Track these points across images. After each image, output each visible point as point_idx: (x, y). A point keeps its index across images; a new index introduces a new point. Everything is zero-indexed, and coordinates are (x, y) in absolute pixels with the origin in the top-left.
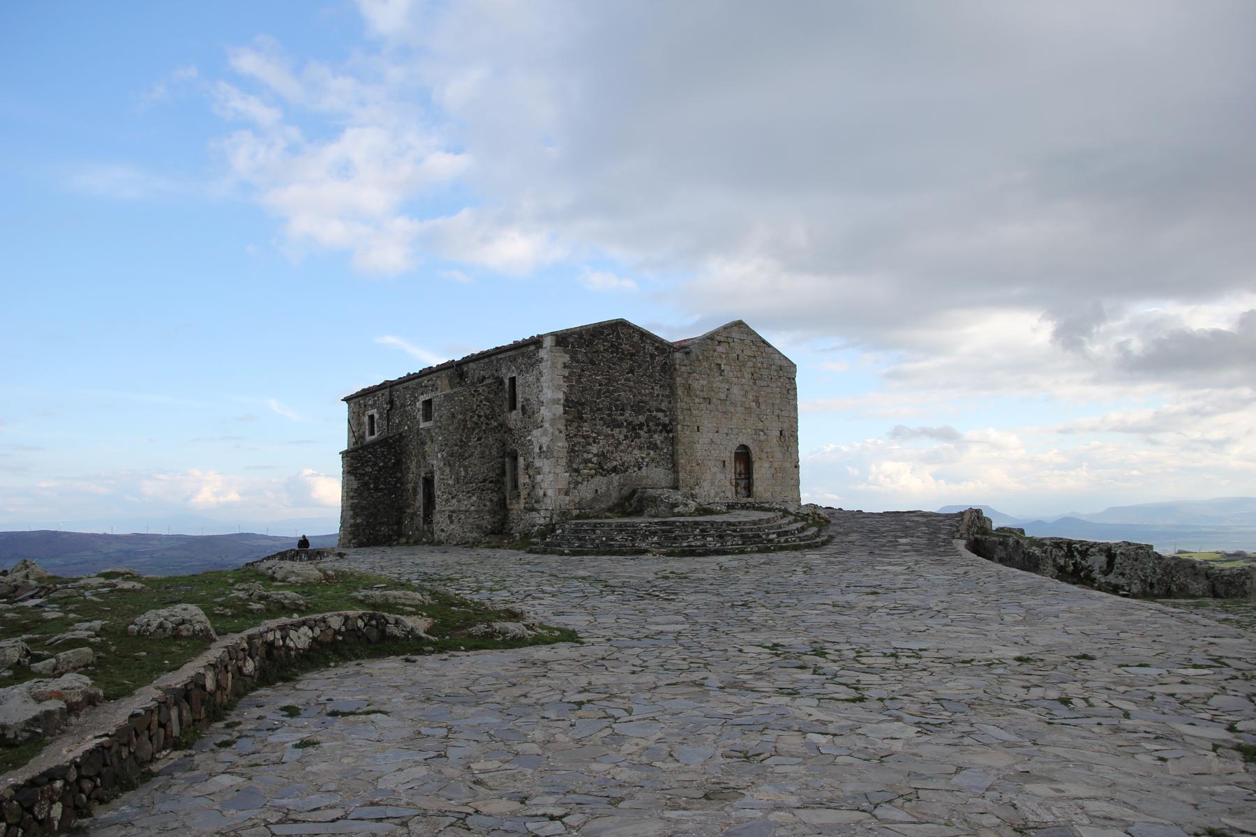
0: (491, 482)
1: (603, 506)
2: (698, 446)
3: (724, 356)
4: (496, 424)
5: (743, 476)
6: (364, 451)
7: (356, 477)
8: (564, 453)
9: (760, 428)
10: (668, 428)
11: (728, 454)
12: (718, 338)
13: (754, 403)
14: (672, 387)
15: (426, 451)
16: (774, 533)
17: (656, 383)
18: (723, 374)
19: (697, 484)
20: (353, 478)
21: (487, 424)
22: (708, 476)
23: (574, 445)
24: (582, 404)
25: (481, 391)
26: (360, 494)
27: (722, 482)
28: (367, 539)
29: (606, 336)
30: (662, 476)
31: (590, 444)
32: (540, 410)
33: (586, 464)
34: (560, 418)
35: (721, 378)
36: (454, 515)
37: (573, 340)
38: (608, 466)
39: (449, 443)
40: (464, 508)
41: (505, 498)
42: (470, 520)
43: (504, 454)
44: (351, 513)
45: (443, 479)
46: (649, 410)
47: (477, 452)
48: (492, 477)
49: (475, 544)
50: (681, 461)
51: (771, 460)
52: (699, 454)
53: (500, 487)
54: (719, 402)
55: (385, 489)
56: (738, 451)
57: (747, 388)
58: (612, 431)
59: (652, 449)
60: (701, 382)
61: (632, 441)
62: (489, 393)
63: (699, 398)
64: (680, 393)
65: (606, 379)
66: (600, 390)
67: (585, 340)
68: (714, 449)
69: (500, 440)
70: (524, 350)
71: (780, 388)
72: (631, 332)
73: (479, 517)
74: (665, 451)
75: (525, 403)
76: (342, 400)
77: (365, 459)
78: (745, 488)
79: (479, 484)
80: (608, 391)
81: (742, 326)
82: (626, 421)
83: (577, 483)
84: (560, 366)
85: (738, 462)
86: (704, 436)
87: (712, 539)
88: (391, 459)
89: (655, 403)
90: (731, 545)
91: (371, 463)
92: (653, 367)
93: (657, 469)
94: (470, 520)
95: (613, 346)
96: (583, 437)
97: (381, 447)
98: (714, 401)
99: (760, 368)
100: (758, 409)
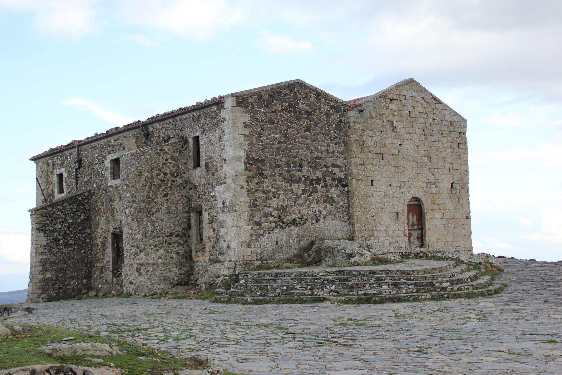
0: (178, 236)
1: (283, 257)
2: (372, 199)
3: (396, 113)
4: (181, 181)
5: (416, 227)
6: (53, 208)
7: (45, 233)
8: (246, 208)
9: (432, 181)
10: (344, 183)
11: (401, 206)
12: (391, 96)
13: (426, 158)
14: (346, 144)
15: (114, 208)
16: (447, 281)
17: (331, 140)
19: (372, 235)
20: (42, 234)
21: (173, 181)
22: (382, 227)
23: (255, 200)
24: (263, 161)
25: (166, 150)
26: (50, 250)
27: (396, 233)
28: (56, 293)
29: (283, 97)
30: (339, 228)
31: (271, 199)
32: (222, 167)
33: (267, 217)
34: (241, 174)
36: (143, 268)
37: (252, 101)
38: (289, 218)
39: (137, 200)
40: (151, 261)
41: (191, 251)
42: (158, 273)
43: (189, 209)
44: (41, 268)
45: (131, 234)
46: (325, 166)
47: (163, 208)
48: (179, 231)
49: (164, 295)
50: (357, 213)
51: (443, 211)
52: (373, 207)
53: (186, 241)
54: (392, 157)
55: (75, 244)
56: (410, 203)
57: (418, 143)
58: (291, 186)
61: (310, 195)
62: (174, 151)
63: (373, 154)
64: (354, 149)
65: (284, 137)
66: (279, 148)
67: (264, 100)
68: (388, 202)
69: (185, 196)
70: (207, 110)
72: (307, 92)
73: (166, 269)
74: (341, 204)
75: (208, 161)
76: (30, 160)
77: (55, 216)
78: (418, 238)
79: (166, 238)
80: (286, 148)
81: (414, 84)
82: (304, 176)
83: (259, 235)
84: (241, 125)
85: (410, 214)
87: (386, 287)
88: (80, 216)
89: (330, 159)
90: (406, 293)
91: (61, 220)
92: (328, 125)
93: (334, 221)
94: (158, 273)
95: (290, 105)
96: (264, 192)
97: (69, 204)
98: (387, 156)
99: (431, 124)
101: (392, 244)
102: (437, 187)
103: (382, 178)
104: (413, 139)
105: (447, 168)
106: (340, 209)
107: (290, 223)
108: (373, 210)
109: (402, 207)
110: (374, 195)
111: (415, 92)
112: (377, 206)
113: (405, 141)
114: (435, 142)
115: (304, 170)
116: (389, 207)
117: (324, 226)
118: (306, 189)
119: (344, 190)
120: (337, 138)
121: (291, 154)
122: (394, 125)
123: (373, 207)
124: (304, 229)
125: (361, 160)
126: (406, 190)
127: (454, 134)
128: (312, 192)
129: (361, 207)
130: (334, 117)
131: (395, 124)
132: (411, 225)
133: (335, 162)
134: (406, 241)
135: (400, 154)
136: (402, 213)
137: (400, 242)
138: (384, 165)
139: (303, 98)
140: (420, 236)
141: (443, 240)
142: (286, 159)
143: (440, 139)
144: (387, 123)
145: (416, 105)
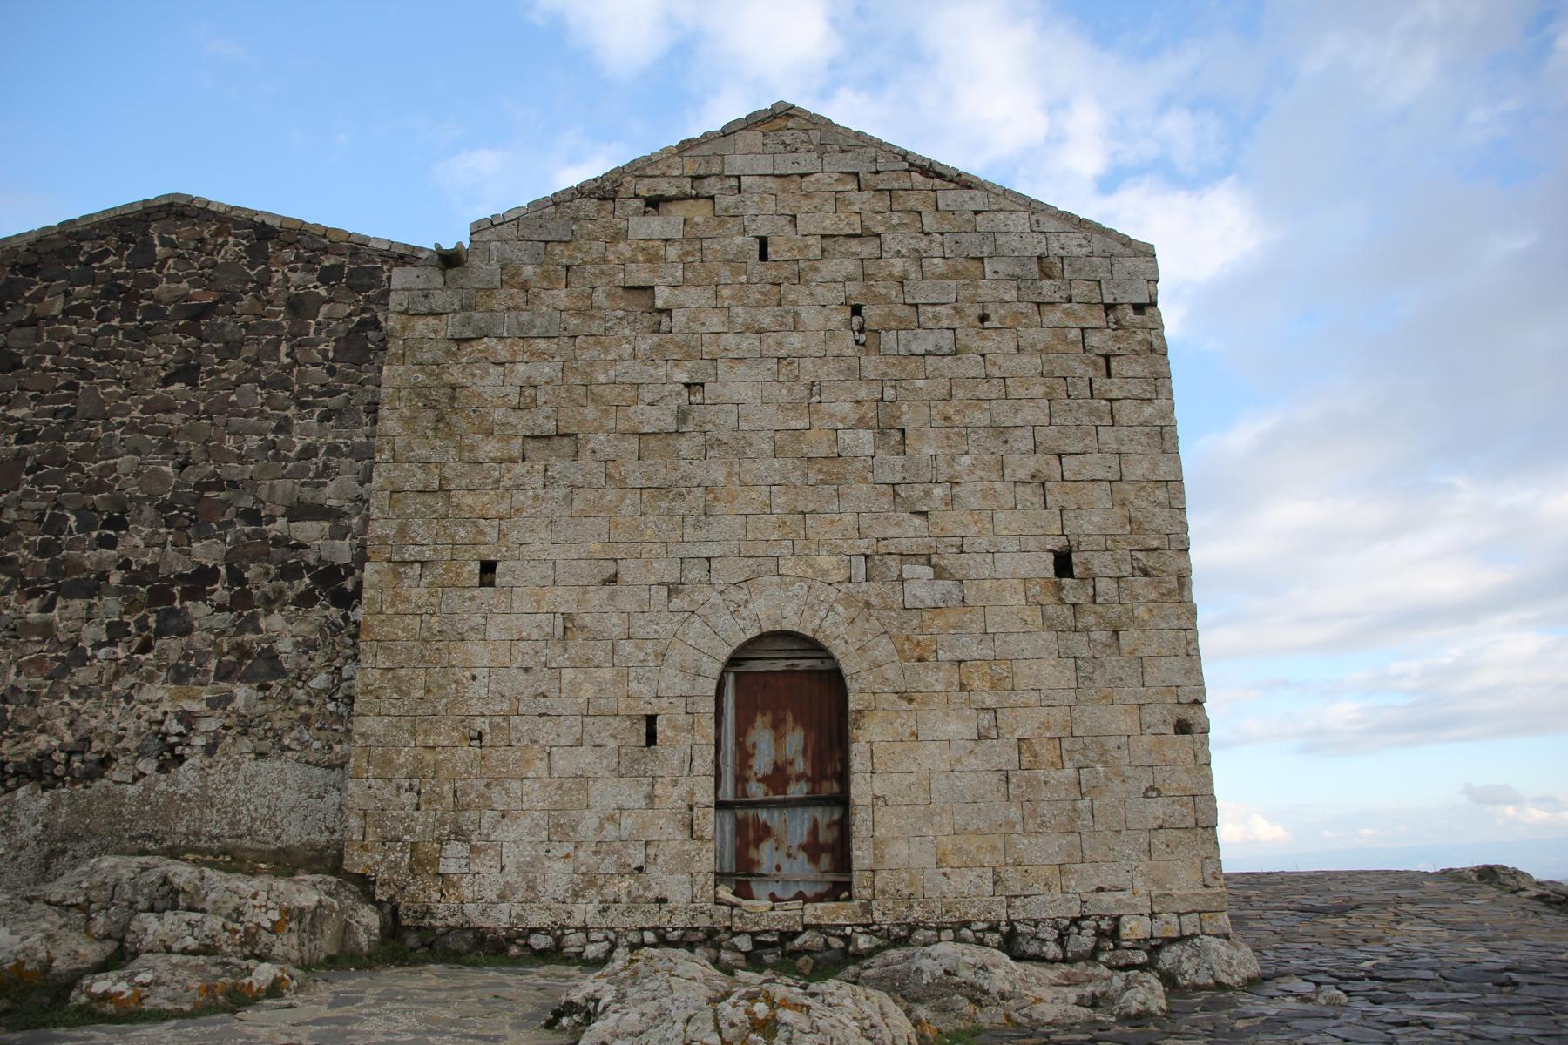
5: (797, 790)
9: (906, 546)
11: (674, 682)
13: (866, 436)
17: (302, 405)
19: (459, 834)
22: (533, 792)
27: (628, 822)
29: (87, 263)
30: (289, 797)
35: (648, 342)
46: (252, 517)
51: (990, 700)
57: (809, 369)
58: (48, 607)
59: (245, 679)
60: (521, 368)
61: (145, 648)
65: (55, 414)
68: (585, 664)
71: (1046, 351)
72: (206, 234)
74: (320, 681)
78: (813, 849)
80: (56, 457)
82: (125, 565)
85: (761, 721)
89: (283, 486)
92: (293, 348)
95: (113, 290)
98: (599, 441)
100: (899, 460)
101: (592, 883)
102: (952, 577)
103: (557, 548)
104: (782, 353)
105: (1022, 474)
106: (311, 704)
107: (16, 774)
108: (477, 707)
110: (493, 633)
111: (802, 157)
112: (506, 688)
113: (721, 365)
114: (930, 360)
115: (134, 540)
116: (588, 690)
117: (205, 787)
118: (126, 618)
119: (346, 618)
120: (339, 393)
121: (75, 480)
122: (659, 304)
123: (479, 689)
124: (83, 803)
125: (429, 473)
126: (716, 598)
127: (1066, 313)
128: (160, 633)
129: (399, 690)
130: (338, 311)
131: (662, 296)
132: (765, 780)
133: (307, 495)
134: (697, 866)
136: (682, 719)
138: (573, 487)
139: (180, 256)
140: (825, 836)
141: (987, 859)
142: (43, 499)
143: (964, 340)
144: (610, 296)
145: (806, 205)
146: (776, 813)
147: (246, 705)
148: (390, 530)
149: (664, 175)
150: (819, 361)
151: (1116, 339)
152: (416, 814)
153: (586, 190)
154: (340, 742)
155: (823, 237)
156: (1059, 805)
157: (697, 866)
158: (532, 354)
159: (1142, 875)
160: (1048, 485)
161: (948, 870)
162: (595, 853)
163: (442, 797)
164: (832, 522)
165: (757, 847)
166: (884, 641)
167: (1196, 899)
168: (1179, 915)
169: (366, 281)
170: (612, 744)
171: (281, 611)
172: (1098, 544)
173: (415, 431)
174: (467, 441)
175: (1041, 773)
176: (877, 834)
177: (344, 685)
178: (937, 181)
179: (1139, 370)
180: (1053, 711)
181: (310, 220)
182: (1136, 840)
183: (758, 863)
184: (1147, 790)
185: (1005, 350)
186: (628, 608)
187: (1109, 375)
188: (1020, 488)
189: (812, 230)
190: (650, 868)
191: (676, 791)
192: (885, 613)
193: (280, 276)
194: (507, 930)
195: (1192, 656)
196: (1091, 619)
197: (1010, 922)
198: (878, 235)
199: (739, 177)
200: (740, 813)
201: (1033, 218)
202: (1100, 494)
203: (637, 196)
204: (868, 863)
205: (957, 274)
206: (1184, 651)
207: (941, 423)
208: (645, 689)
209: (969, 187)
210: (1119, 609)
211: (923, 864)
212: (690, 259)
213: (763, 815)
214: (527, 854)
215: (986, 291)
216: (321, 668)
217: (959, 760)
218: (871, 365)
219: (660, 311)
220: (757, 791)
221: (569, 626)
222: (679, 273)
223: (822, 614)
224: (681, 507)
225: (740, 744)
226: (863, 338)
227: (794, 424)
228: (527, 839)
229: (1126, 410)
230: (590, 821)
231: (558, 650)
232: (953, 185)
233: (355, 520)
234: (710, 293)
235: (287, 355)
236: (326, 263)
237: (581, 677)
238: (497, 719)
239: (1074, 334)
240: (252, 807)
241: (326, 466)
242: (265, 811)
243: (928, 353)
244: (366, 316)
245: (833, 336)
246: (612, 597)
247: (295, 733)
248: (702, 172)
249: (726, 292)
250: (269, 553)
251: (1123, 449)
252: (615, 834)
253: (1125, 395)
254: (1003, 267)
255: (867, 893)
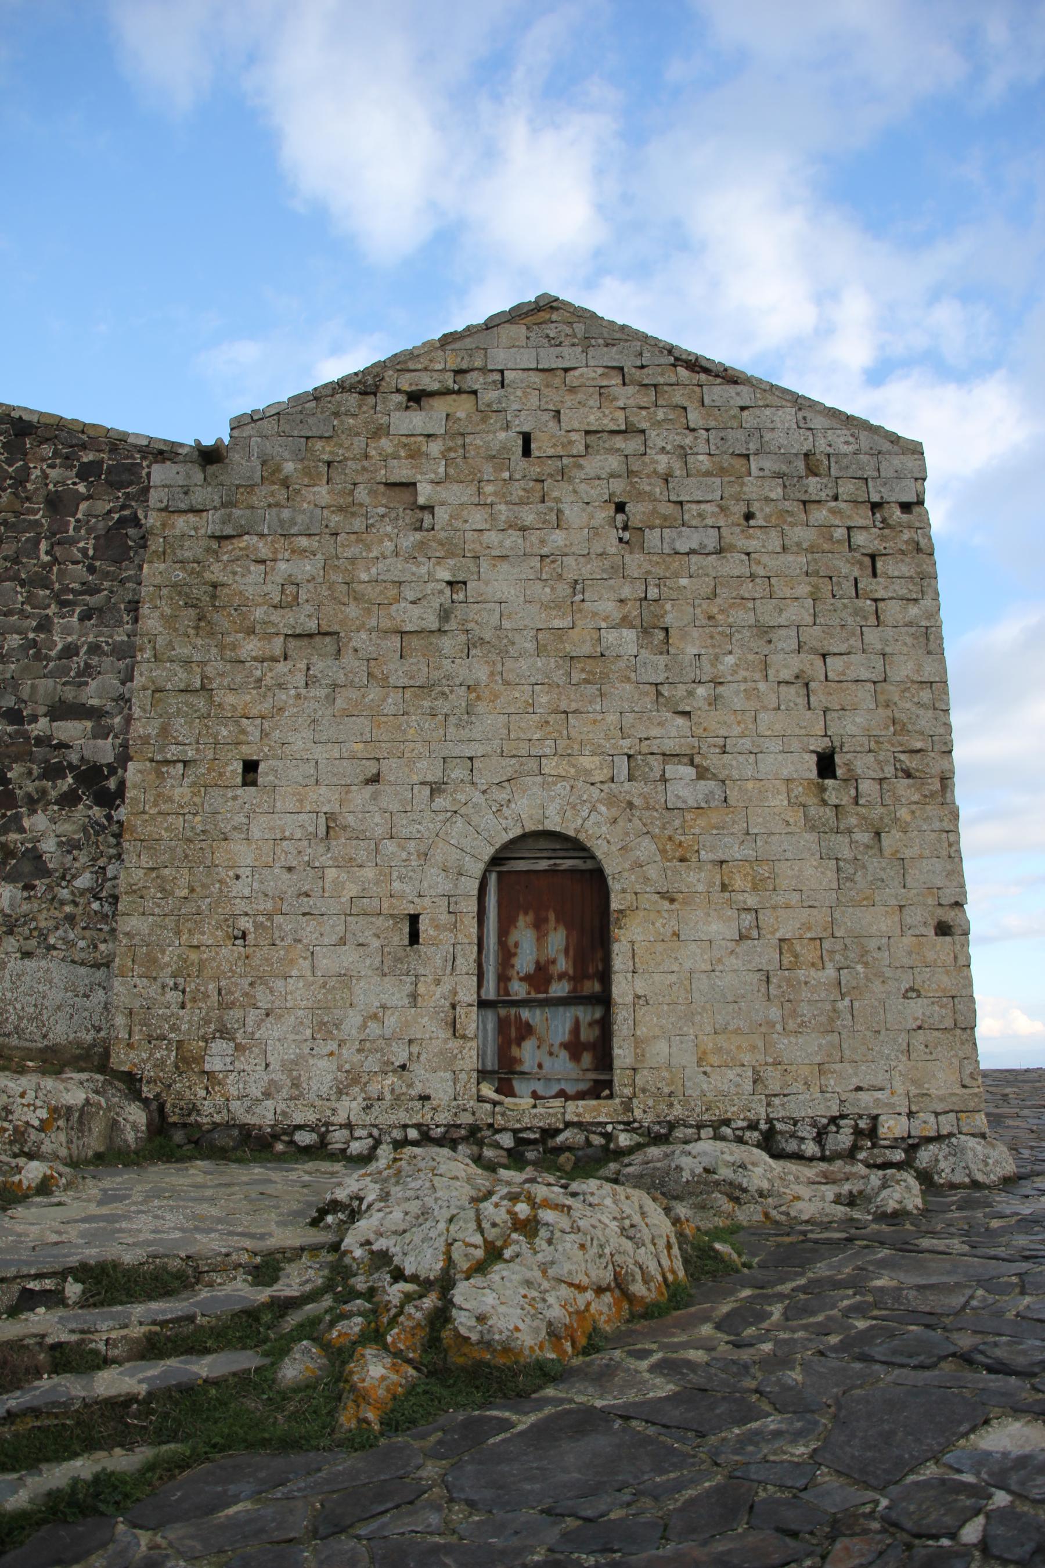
5: (559, 989)
11: (436, 882)
12: (406, 382)
13: (629, 635)
17: (63, 604)
18: (427, 519)
19: (224, 1033)
27: (391, 1021)
30: (56, 996)
35: (410, 540)
51: (751, 901)
57: (572, 568)
60: (282, 566)
68: (348, 863)
71: (811, 550)
74: (84, 881)
78: (574, 1048)
85: (523, 921)
86: (285, 802)
89: (46, 685)
92: (52, 545)
93: (30, 964)
98: (361, 639)
100: (662, 659)
101: (355, 1081)
104: (545, 551)
105: (786, 675)
106: (76, 904)
108: (241, 906)
109: (444, 885)
110: (256, 833)
111: (566, 351)
112: (270, 887)
113: (485, 564)
114: (694, 558)
116: (352, 890)
119: (109, 817)
120: (99, 591)
122: (421, 501)
123: (241, 888)
125: (190, 672)
126: (478, 798)
127: (833, 511)
129: (163, 890)
131: (425, 493)
132: (527, 979)
133: (69, 694)
134: (459, 1064)
135: (452, 625)
136: (444, 918)
137: (417, 1070)
138: (335, 686)
140: (587, 1035)
141: (747, 1058)
144: (372, 493)
145: (569, 400)
146: (538, 1012)
147: (11, 905)
148: (152, 730)
149: (426, 369)
150: (582, 559)
151: (883, 538)
152: (181, 1012)
153: (347, 385)
154: (105, 941)
155: (587, 432)
156: (819, 1005)
157: (459, 1064)
158: (293, 552)
159: (901, 1075)
160: (812, 685)
161: (708, 1069)
162: (359, 1051)
163: (206, 996)
164: (595, 721)
165: (519, 1045)
166: (646, 841)
167: (954, 1099)
168: (937, 1114)
169: (125, 477)
170: (376, 943)
171: (44, 811)
172: (862, 745)
173: (176, 630)
174: (228, 639)
175: (801, 974)
176: (638, 1033)
177: (109, 884)
178: (703, 377)
179: (905, 569)
180: (815, 912)
181: (68, 415)
182: (895, 1040)
183: (520, 1062)
184: (907, 991)
185: (770, 548)
186: (391, 807)
187: (875, 575)
188: (783, 688)
189: (576, 426)
190: (413, 1066)
191: (439, 991)
192: (647, 813)
193: (38, 472)
194: (272, 1126)
195: (954, 857)
196: (853, 821)
197: (769, 1121)
198: (643, 431)
199: (502, 372)
200: (503, 1012)
201: (800, 415)
202: (864, 695)
203: (398, 391)
204: (629, 1061)
205: (722, 471)
206: (945, 853)
207: (705, 622)
208: (408, 888)
209: (736, 383)
210: (881, 810)
211: (684, 1063)
212: (453, 455)
213: (525, 1014)
214: (291, 1052)
215: (751, 488)
216: (85, 868)
217: (720, 960)
218: (635, 563)
219: (423, 508)
220: (519, 990)
221: (332, 826)
222: (442, 470)
223: (585, 814)
224: (443, 706)
225: (502, 943)
226: (627, 536)
227: (557, 623)
228: (291, 1037)
229: (892, 611)
230: (353, 1020)
231: (321, 849)
232: (719, 381)
233: (117, 720)
234: (472, 489)
235: (47, 553)
236: (85, 460)
237: (344, 876)
238: (261, 919)
239: (840, 533)
240: (19, 1006)
241: (88, 666)
242: (32, 1010)
243: (693, 552)
244: (126, 513)
245: (596, 534)
246: (375, 797)
247: (60, 933)
248: (464, 366)
249: (489, 489)
250: (31, 753)
251: (888, 650)
252: (378, 1032)
253: (891, 595)
254: (769, 464)
255: (628, 1091)
